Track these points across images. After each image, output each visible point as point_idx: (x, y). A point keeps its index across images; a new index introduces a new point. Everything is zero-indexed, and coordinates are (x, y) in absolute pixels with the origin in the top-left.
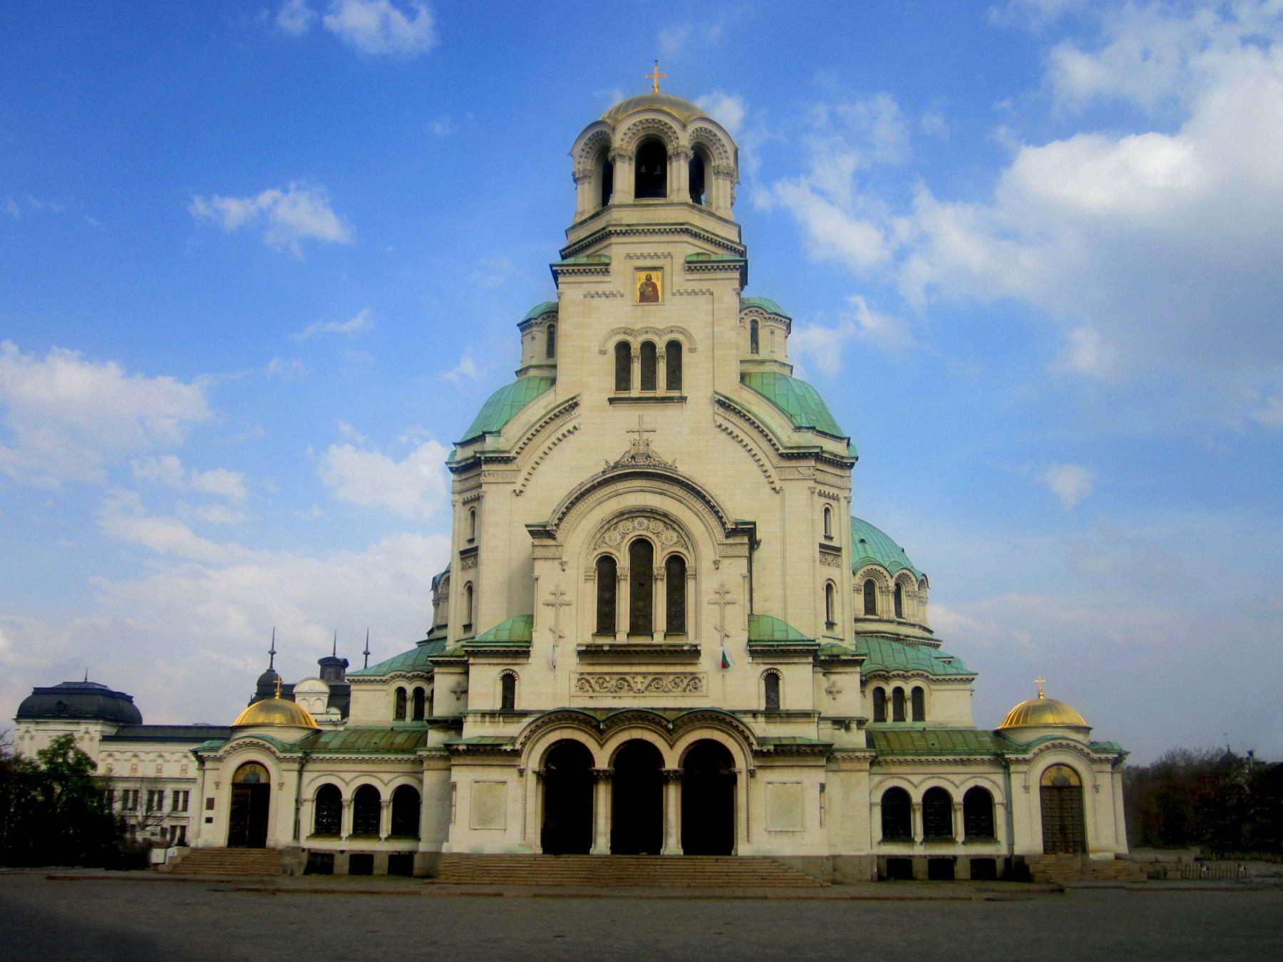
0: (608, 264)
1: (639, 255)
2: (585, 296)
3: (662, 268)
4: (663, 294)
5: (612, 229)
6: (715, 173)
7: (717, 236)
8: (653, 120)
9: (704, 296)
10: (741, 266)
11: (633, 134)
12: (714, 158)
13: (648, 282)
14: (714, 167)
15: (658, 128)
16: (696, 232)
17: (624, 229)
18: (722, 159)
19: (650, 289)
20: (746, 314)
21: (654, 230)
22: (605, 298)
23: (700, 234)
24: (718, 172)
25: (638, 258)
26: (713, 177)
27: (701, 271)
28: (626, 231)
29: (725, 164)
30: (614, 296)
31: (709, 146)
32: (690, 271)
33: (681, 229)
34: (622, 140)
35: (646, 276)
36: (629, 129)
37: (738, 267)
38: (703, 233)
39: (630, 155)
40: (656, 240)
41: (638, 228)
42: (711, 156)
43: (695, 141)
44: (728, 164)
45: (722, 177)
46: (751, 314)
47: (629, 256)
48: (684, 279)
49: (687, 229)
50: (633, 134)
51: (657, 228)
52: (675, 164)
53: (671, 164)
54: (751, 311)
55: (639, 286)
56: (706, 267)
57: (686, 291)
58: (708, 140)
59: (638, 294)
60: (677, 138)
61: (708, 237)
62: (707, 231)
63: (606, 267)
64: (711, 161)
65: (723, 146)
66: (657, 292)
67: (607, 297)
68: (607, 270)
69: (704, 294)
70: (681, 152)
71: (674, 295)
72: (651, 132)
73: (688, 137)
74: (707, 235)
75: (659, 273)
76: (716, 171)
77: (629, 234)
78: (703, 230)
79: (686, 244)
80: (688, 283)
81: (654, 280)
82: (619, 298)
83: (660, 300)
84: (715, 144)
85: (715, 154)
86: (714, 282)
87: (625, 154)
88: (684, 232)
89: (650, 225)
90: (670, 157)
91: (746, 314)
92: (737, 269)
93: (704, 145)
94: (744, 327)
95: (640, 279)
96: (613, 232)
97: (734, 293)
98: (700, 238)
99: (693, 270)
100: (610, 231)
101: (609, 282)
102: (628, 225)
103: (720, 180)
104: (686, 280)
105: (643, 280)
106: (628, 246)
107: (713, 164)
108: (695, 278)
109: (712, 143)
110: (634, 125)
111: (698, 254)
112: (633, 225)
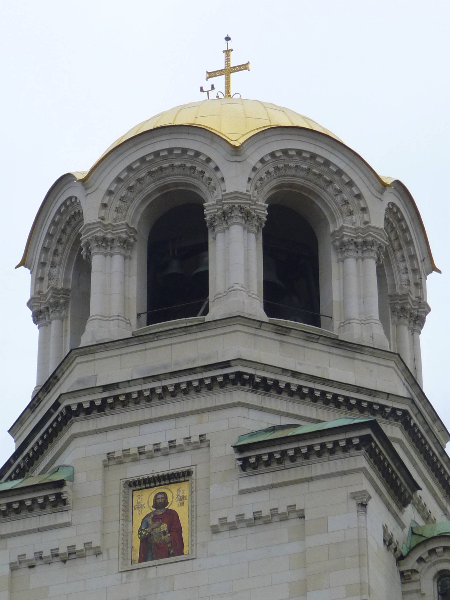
0: (61, 484)
1: (134, 451)
2: (14, 568)
3: (189, 473)
4: (191, 531)
5: (73, 402)
6: (336, 248)
7: (325, 381)
8: (171, 151)
9: (285, 524)
10: (365, 440)
11: (130, 189)
12: (332, 214)
13: (160, 512)
14: (333, 234)
15: (183, 166)
16: (264, 379)
17: (98, 397)
18: (351, 213)
19: (164, 527)
20: (421, 560)
21: (165, 388)
22: (60, 564)
23: (276, 382)
24: (343, 244)
25: (135, 460)
26: (334, 257)
27: (275, 466)
28: (104, 400)
29: (359, 224)
30: (81, 555)
31: (317, 189)
32: (249, 470)
33: (226, 376)
34: (105, 206)
35: (156, 498)
36: (118, 180)
37: (356, 441)
38: (284, 379)
39: (124, 236)
40: (172, 412)
41: (128, 390)
42: (326, 213)
43: (274, 183)
44: (366, 223)
45: (351, 253)
46: (434, 558)
47: (110, 456)
48: (236, 490)
49: (239, 374)
50: (130, 189)
51: (170, 382)
52: (220, 236)
53: (215, 238)
54: (432, 552)
55: (137, 524)
56: (284, 453)
57: (240, 518)
58: (311, 177)
59: (137, 543)
60: (223, 179)
61: (300, 388)
62: (295, 374)
63: (57, 491)
64: (327, 224)
65: (351, 184)
66: (180, 531)
67: (64, 561)
68: (58, 496)
69: (284, 518)
70: (232, 209)
71: (215, 530)
72: (170, 180)
73: (248, 173)
74: (295, 382)
75: (185, 487)
76: (337, 243)
77: (112, 407)
78: (284, 371)
79: (239, 411)
80: (248, 499)
81: (173, 505)
82: (91, 559)
83: (186, 549)
84: (330, 183)
85: (334, 207)
86: (305, 485)
87: (109, 236)
88: (234, 383)
89: (156, 378)
90: (211, 224)
91: (421, 560)
92: (358, 448)
93: (301, 188)
94: (418, 591)
95: (141, 507)
96: (74, 408)
97: (353, 505)
98: (280, 391)
99: (255, 467)
100: (68, 408)
101: (67, 525)
102: (106, 388)
103: (351, 263)
104: (243, 492)
105: (148, 510)
106: (111, 435)
107: (332, 228)
108: (260, 484)
109: (322, 183)
110: (129, 169)
111: (274, 429)
112: (116, 386)
